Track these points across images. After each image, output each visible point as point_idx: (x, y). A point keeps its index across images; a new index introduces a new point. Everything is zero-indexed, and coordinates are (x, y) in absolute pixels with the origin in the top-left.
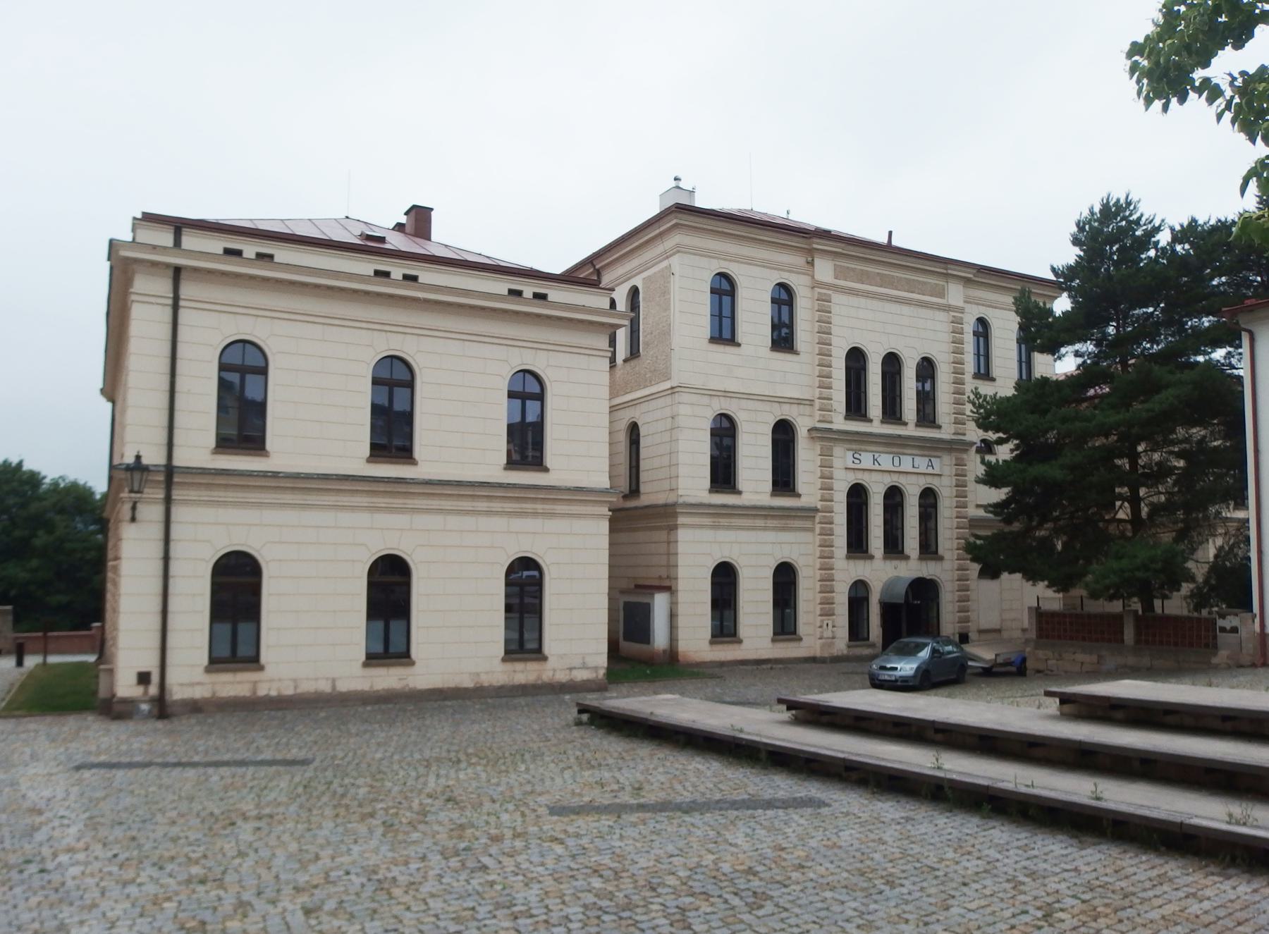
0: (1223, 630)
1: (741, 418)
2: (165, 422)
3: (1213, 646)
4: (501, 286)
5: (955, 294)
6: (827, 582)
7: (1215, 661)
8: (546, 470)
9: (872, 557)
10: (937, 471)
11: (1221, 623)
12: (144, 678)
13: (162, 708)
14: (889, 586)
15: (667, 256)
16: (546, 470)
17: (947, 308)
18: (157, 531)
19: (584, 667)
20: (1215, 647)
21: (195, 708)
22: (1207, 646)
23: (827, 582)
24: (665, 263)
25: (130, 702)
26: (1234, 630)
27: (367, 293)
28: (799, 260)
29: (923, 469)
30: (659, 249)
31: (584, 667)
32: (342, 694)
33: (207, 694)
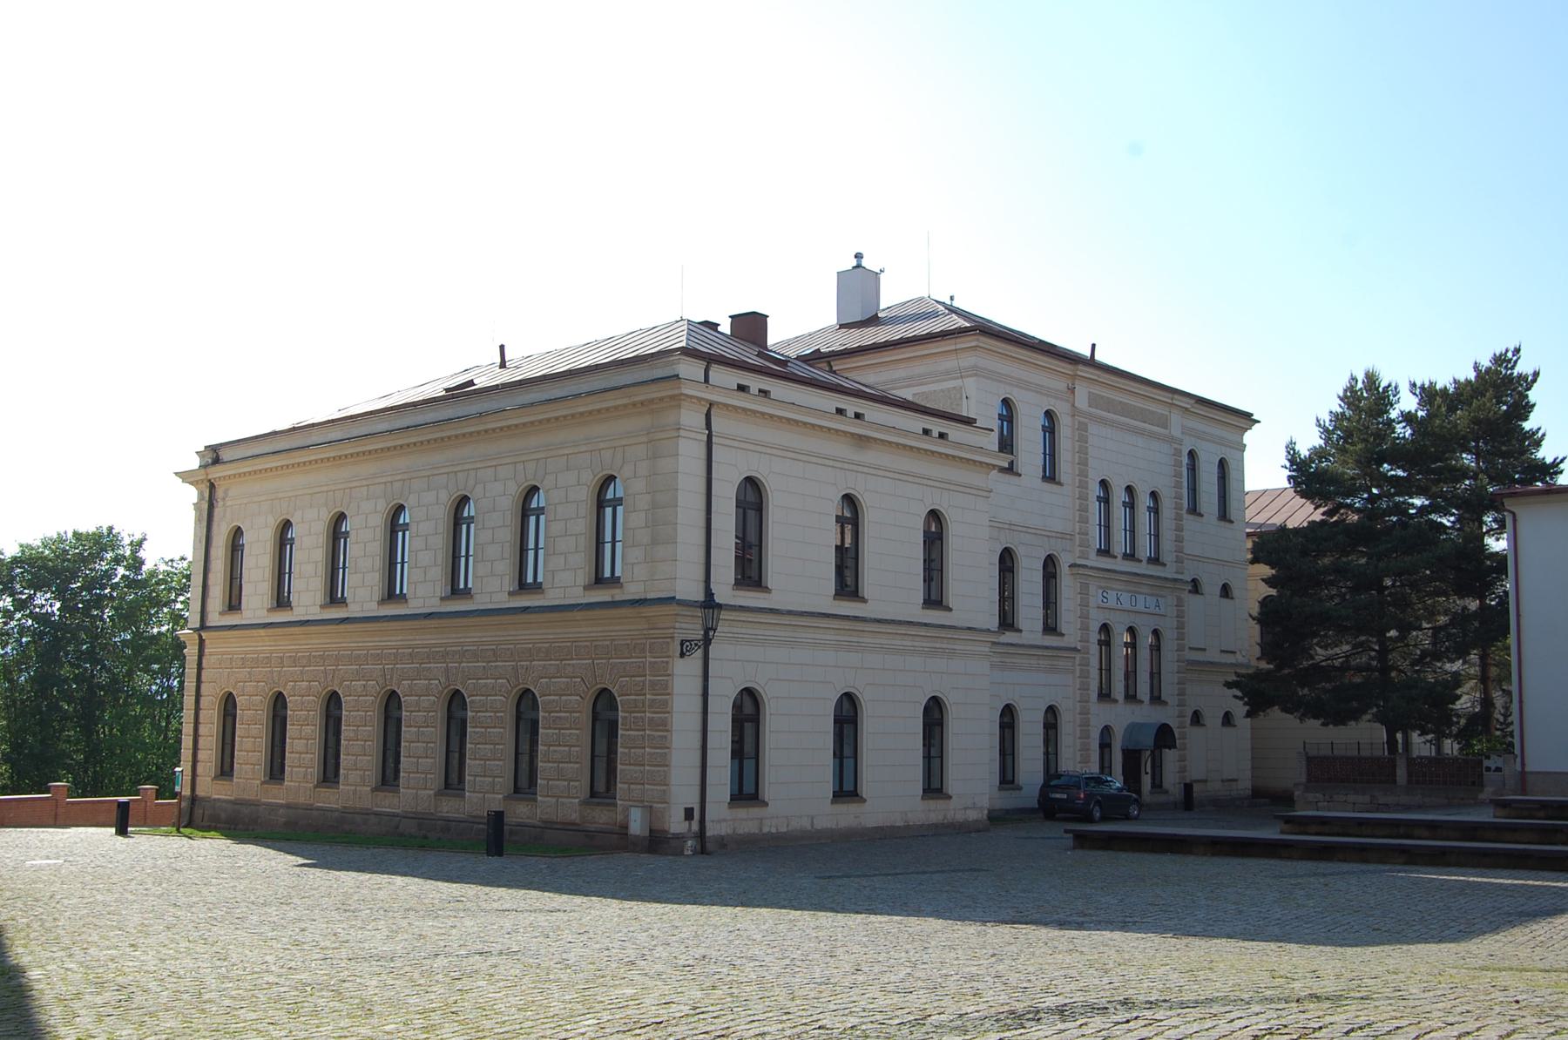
0: (1488, 769)
1: (1020, 552)
2: (702, 560)
3: (1479, 784)
4: (916, 423)
5: (1177, 422)
6: (1085, 724)
7: (1482, 796)
8: (767, 590)
9: (1116, 701)
10: (1162, 611)
11: (1486, 763)
12: (689, 813)
13: (704, 845)
14: (1132, 729)
15: (961, 374)
16: (767, 590)
17: (1171, 440)
18: (699, 664)
19: (974, 807)
20: (1482, 785)
21: (722, 843)
22: (1473, 783)
23: (1085, 724)
24: (958, 383)
25: (679, 837)
26: (1498, 769)
27: (745, 410)
28: (1061, 385)
29: (1127, 606)
30: (950, 363)
31: (974, 807)
32: (818, 831)
33: (730, 831)
